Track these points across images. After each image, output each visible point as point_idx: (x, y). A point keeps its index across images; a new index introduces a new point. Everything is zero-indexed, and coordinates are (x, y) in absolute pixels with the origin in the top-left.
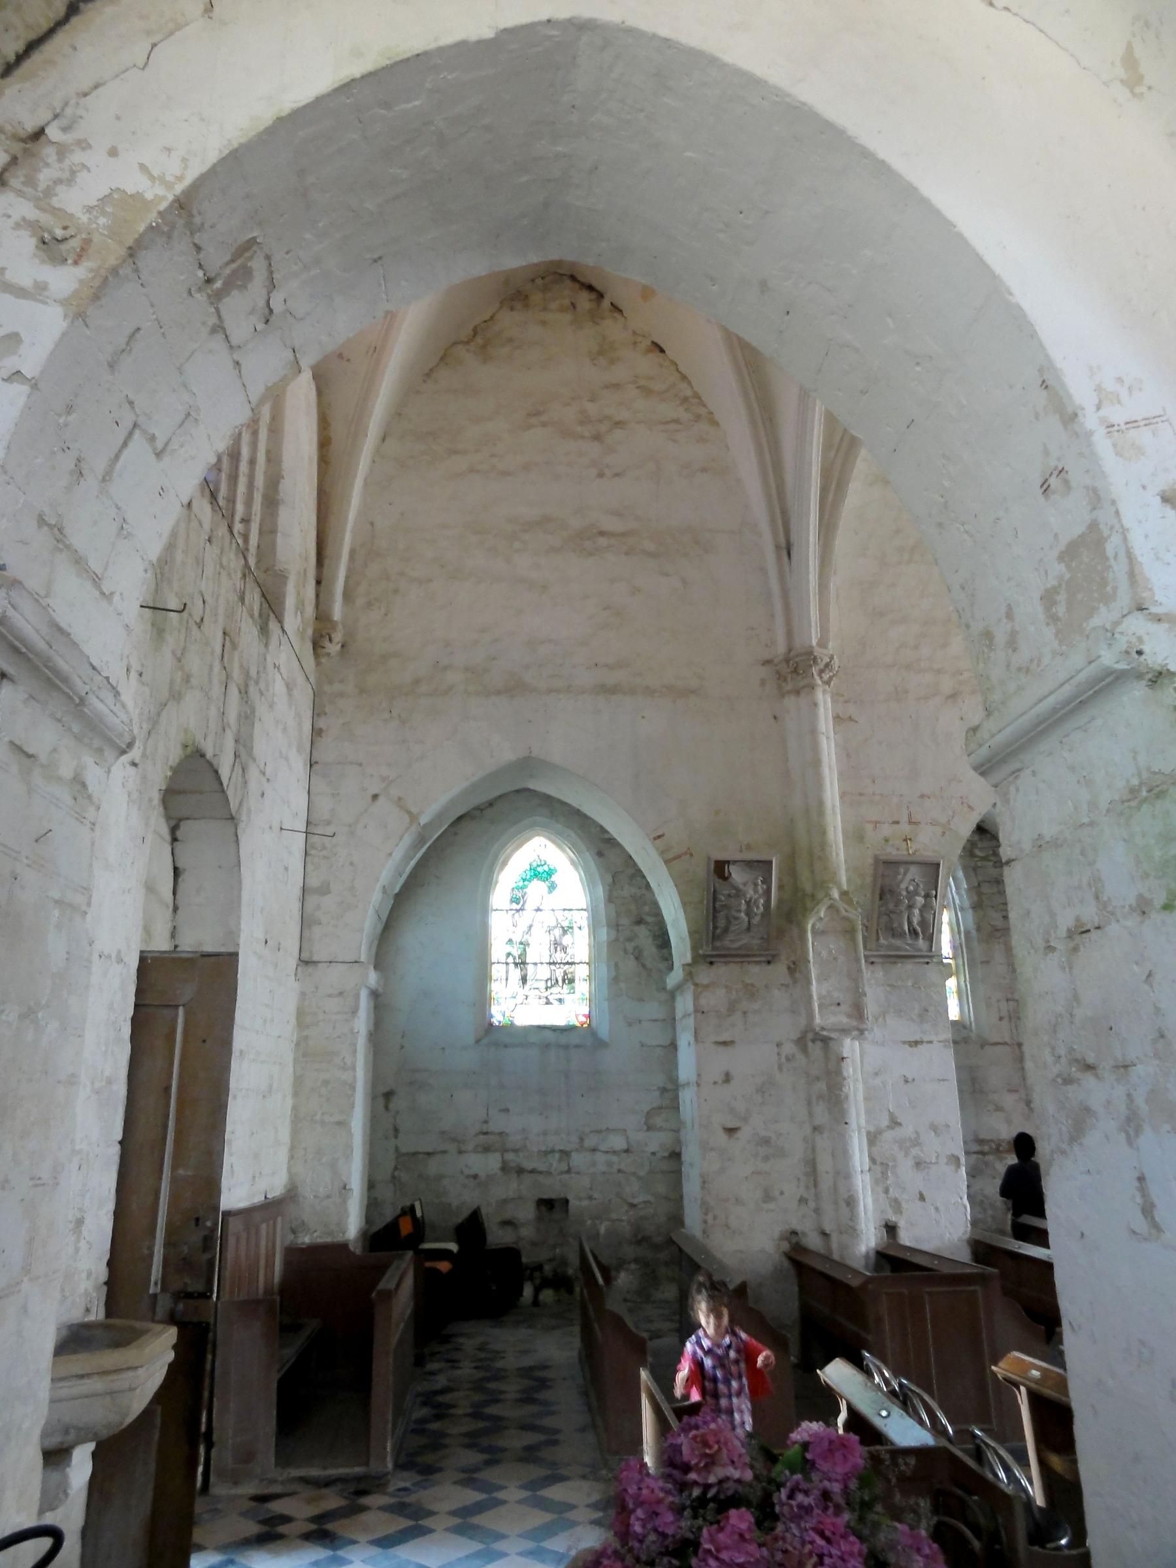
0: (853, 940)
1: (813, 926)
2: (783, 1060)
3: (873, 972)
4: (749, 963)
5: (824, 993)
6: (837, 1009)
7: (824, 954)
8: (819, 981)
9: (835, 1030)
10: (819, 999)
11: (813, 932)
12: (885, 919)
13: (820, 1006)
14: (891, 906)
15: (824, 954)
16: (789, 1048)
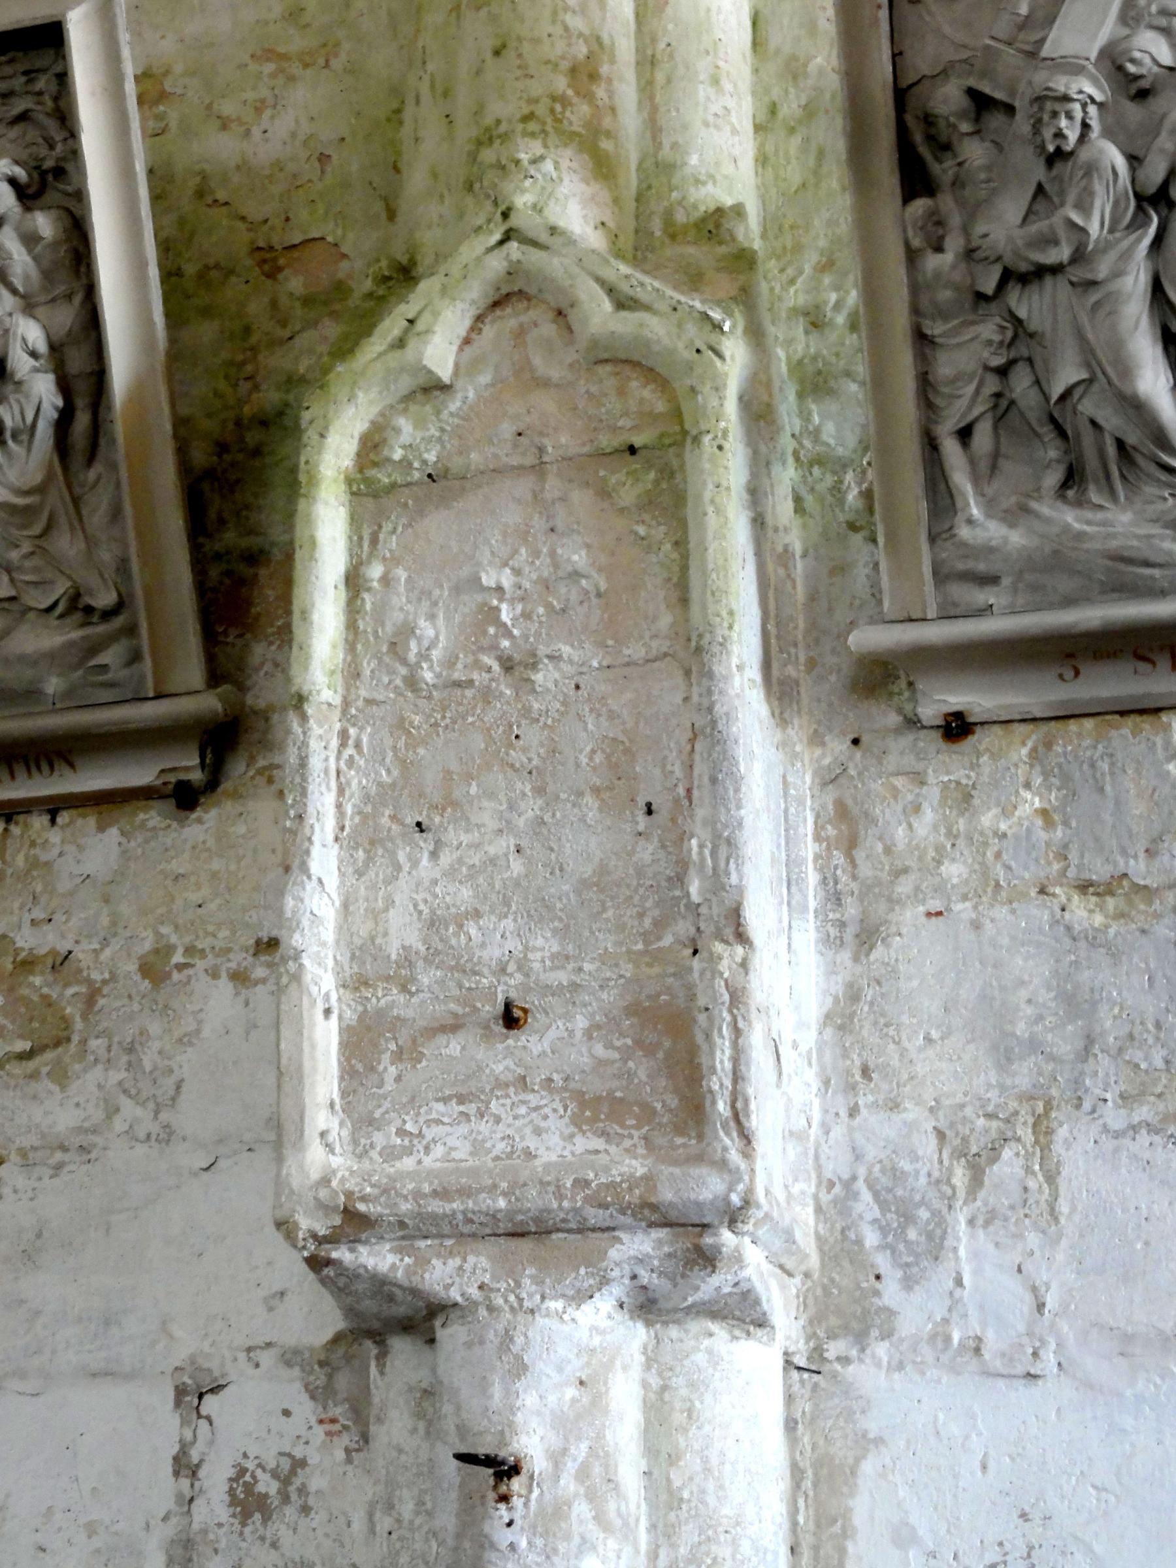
0: (670, 502)
1: (371, 447)
2: (214, 1507)
3: (963, 798)
4: (53, 808)
5: (402, 932)
6: (500, 1057)
7: (435, 634)
8: (364, 841)
9: (469, 1232)
10: (356, 983)
11: (369, 489)
12: (970, 349)
13: (361, 1046)
14: (1004, 225)
15: (435, 634)
16: (262, 1417)
